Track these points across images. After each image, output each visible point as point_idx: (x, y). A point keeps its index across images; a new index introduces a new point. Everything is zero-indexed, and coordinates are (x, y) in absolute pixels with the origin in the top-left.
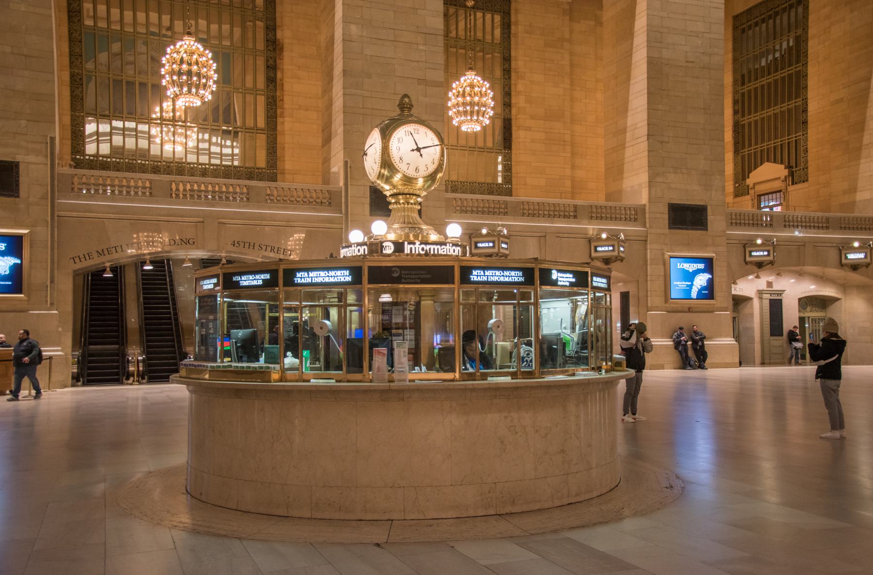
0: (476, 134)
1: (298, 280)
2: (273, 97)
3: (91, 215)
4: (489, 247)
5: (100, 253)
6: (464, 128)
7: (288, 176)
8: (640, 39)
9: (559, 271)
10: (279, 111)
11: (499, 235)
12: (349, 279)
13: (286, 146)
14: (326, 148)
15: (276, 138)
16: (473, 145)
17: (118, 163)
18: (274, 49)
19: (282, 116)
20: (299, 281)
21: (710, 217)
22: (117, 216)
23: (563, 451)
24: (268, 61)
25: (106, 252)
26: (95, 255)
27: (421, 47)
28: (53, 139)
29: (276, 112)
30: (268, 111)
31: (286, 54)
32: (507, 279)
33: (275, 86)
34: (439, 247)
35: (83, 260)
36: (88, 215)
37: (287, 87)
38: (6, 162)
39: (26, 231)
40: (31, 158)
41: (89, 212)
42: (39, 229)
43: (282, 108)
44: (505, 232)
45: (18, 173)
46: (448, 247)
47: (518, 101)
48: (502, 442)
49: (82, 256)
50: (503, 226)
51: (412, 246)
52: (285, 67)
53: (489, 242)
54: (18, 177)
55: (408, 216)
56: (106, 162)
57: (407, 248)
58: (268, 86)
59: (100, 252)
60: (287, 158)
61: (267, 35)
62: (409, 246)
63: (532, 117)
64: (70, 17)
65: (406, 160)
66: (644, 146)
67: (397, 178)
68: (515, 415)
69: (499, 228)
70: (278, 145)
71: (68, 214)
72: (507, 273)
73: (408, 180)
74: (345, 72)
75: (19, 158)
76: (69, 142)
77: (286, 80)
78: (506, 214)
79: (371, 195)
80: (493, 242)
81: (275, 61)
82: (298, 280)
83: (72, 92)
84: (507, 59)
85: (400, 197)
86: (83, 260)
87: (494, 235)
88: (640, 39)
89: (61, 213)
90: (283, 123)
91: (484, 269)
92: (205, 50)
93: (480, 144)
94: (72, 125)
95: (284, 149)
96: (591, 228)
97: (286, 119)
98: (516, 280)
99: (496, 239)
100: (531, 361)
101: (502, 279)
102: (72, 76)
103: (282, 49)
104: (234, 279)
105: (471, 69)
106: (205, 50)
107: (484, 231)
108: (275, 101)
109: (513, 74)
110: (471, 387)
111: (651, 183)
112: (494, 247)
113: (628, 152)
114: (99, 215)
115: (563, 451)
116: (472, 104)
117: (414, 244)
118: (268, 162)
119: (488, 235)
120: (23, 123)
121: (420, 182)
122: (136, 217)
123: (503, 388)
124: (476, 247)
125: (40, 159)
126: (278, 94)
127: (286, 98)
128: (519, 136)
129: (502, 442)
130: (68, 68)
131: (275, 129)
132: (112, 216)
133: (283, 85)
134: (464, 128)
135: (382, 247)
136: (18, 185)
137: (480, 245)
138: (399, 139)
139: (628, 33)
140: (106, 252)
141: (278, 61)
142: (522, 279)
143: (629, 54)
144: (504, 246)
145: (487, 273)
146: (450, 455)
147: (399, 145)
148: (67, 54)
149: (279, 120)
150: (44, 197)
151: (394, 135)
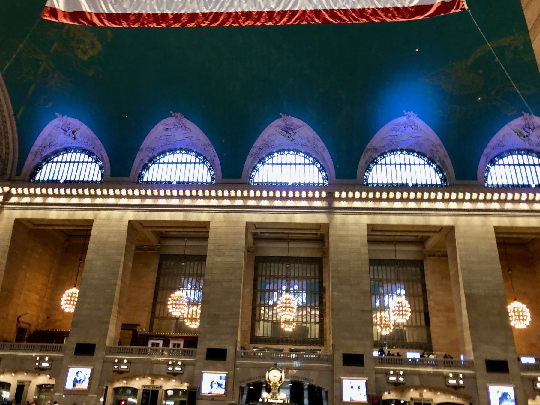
5: (248, 380)
8: (461, 286)
21: (510, 367)
28: (237, 341)
40: (231, 347)
47: (431, 304)
63: (438, 311)
66: (469, 332)
78: (402, 364)
84: (424, 286)
88: (461, 286)
93: (414, 324)
96: (445, 371)
109: (428, 293)
111: (474, 350)
113: (465, 334)
128: (433, 320)
139: (458, 283)
143: (459, 292)
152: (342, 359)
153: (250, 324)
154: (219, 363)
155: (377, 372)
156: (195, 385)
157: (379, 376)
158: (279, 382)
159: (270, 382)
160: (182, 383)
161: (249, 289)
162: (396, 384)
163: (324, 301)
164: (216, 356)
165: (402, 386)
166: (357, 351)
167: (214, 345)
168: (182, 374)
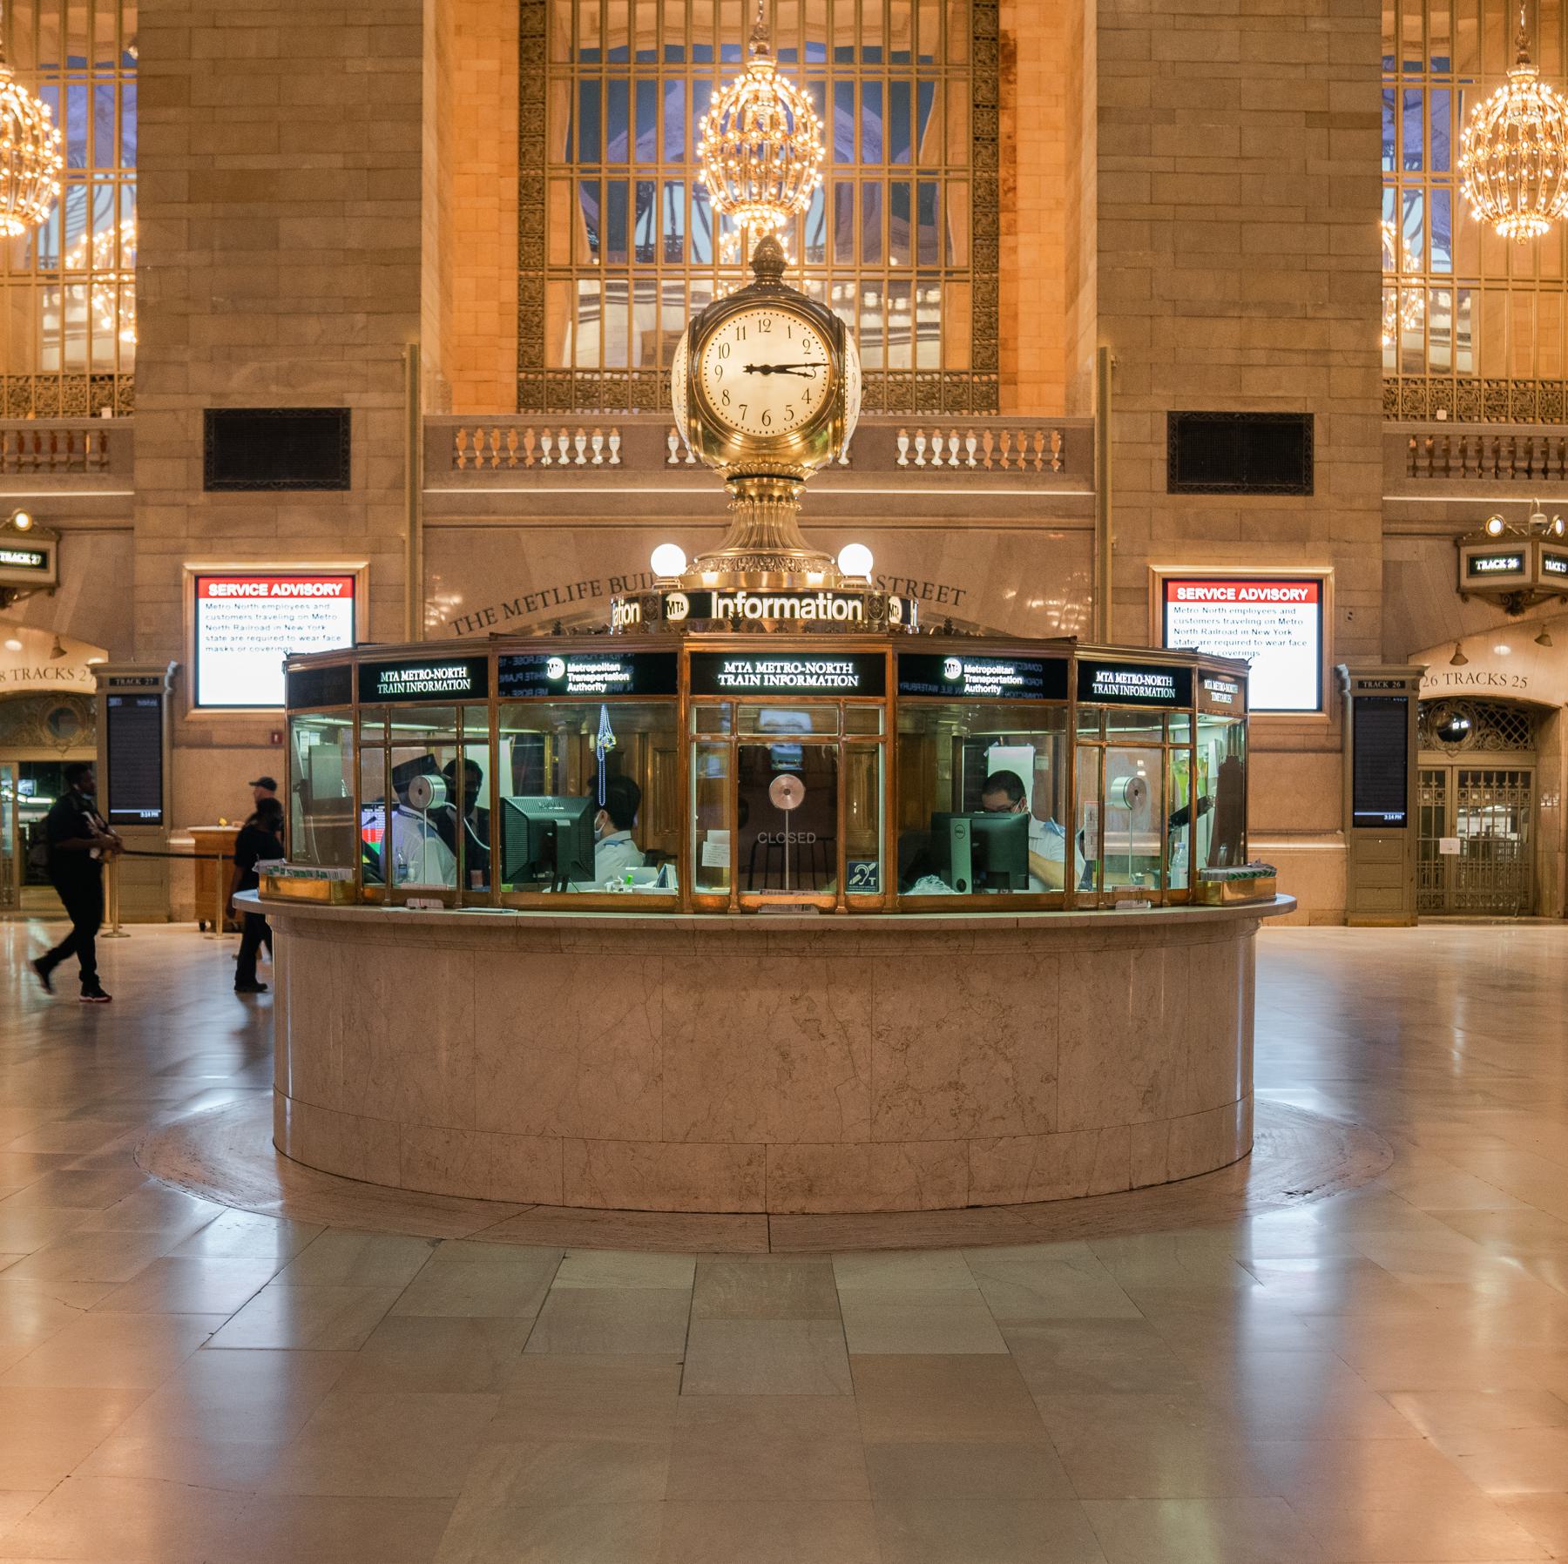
0: (1536, 245)
1: (384, 689)
2: (989, 182)
3: (493, 519)
4: (1506, 572)
5: (511, 610)
6: (1502, 229)
7: (1024, 389)
9: (966, 659)
10: (1004, 219)
11: (1539, 534)
12: (466, 684)
13: (1022, 308)
14: (1071, 313)
15: (996, 289)
16: (1500, 272)
17: (617, 383)
18: (994, 58)
19: (1012, 230)
20: (731, 681)
22: (546, 519)
23: (956, 1086)
24: (976, 90)
25: (523, 607)
26: (500, 614)
27: (1317, 25)
29: (996, 222)
30: (976, 223)
31: (1024, 67)
32: (812, 682)
33: (995, 154)
34: (795, 601)
35: (475, 625)
36: (484, 519)
37: (1023, 155)
38: (326, 411)
39: (361, 565)
40: (374, 399)
41: (487, 512)
42: (385, 557)
43: (1012, 209)
44: (1559, 527)
45: (347, 433)
46: (821, 601)
48: (784, 1056)
49: (473, 618)
50: (1548, 509)
51: (728, 601)
52: (1021, 101)
53: (1507, 556)
54: (348, 443)
55: (770, 527)
56: (591, 382)
57: (717, 608)
58: (976, 155)
59: (511, 605)
60: (1022, 342)
61: (976, 23)
62: (722, 602)
64: (523, 50)
65: (736, 399)
67: (736, 443)
68: (819, 996)
69: (1538, 517)
70: (1001, 309)
71: (446, 520)
72: (813, 667)
73: (765, 445)
74: (1102, 112)
75: (350, 400)
76: (514, 343)
77: (1022, 135)
79: (1170, 437)
80: (1520, 556)
81: (996, 89)
82: (384, 689)
83: (522, 222)
85: (748, 483)
86: (475, 625)
87: (1521, 538)
89: (431, 520)
90: (1014, 250)
91: (753, 657)
92: (799, 90)
94: (521, 302)
95: (1015, 316)
97: (1023, 238)
98: (838, 682)
99: (1527, 547)
100: (874, 873)
101: (800, 681)
102: (523, 185)
103: (1012, 58)
104: (626, 677)
105: (1524, 60)
106: (799, 90)
107: (1495, 527)
108: (994, 193)
110: (689, 927)
112: (1520, 570)
114: (510, 519)
115: (956, 1086)
116: (1534, 161)
117: (733, 596)
118: (975, 354)
119: (1506, 536)
120: (360, 319)
121: (796, 442)
122: (585, 519)
123: (785, 932)
124: (1473, 571)
125: (389, 399)
126: (1002, 173)
127: (1022, 183)
129: (784, 1056)
130: (516, 169)
131: (995, 268)
132: (535, 519)
133: (1014, 149)
134: (1502, 229)
135: (665, 604)
136: (347, 462)
137: (1484, 565)
138: (721, 349)
140: (523, 607)
141: (1003, 88)
142: (853, 681)
144: (1553, 566)
145: (760, 668)
146: (660, 1076)
147: (722, 362)
148: (514, 136)
149: (1005, 241)
150: (397, 485)
151: (712, 340)
152: (1162, 452)
153: (510, 292)
154: (298, 508)
155: (1396, 526)
156: (144, 661)
157: (1404, 550)
158: (812, 427)
159: (713, 434)
160: (59, 652)
161: (491, 65)
162: (1514, 600)
163: (1005, 125)
164: (277, 454)
165: (1553, 606)
166: (1268, 392)
167: (248, 389)
168: (52, 589)
